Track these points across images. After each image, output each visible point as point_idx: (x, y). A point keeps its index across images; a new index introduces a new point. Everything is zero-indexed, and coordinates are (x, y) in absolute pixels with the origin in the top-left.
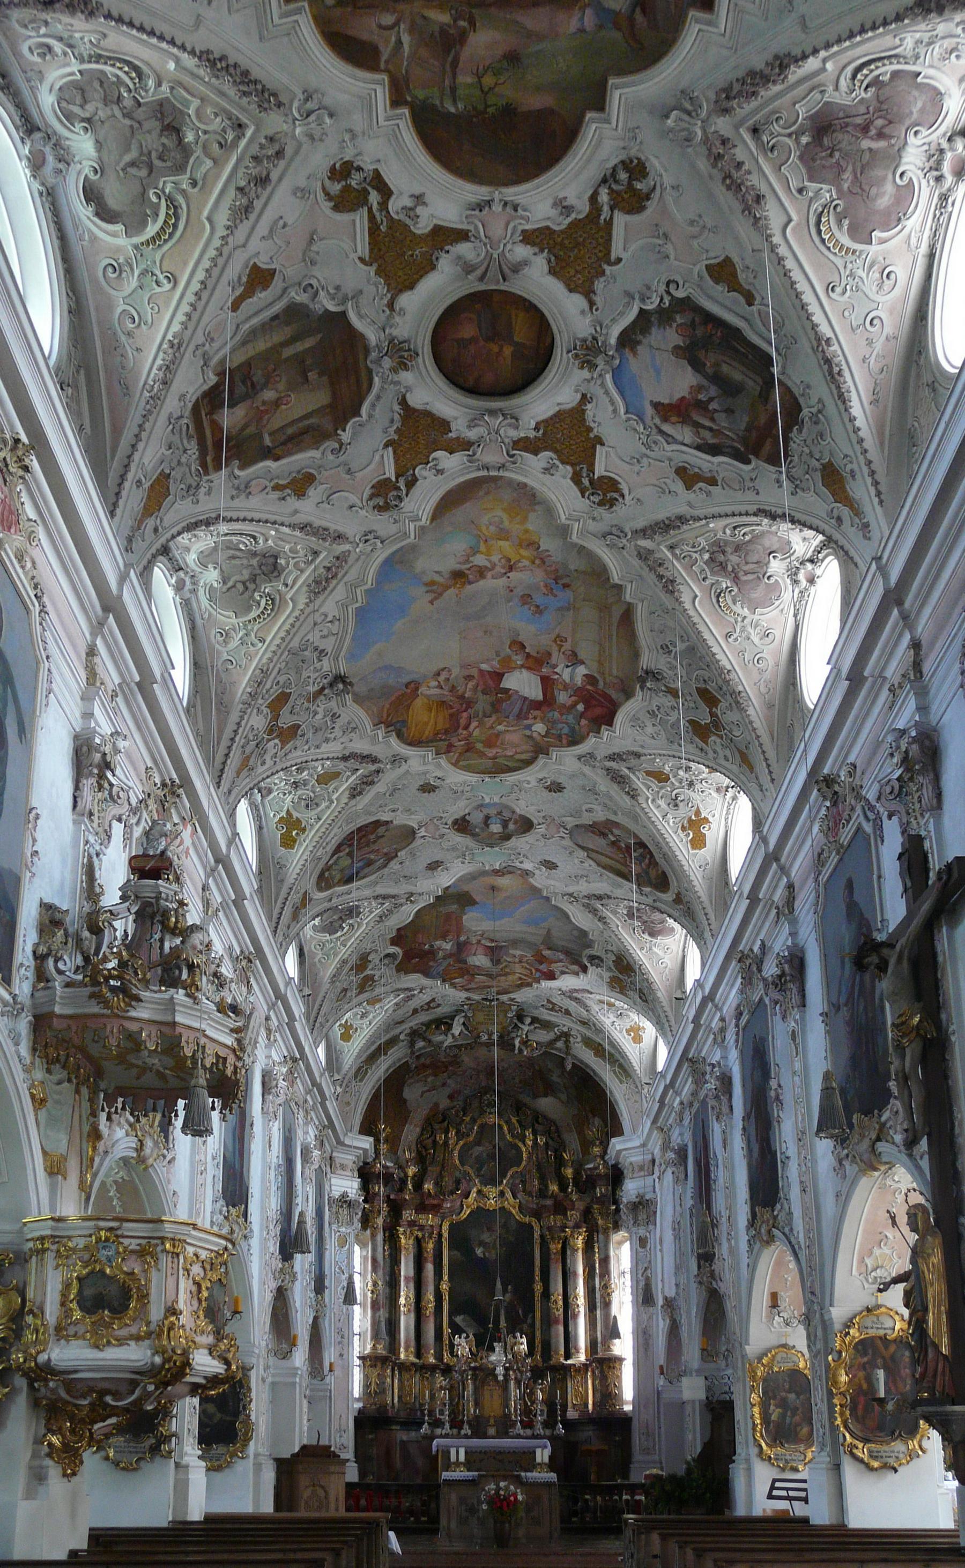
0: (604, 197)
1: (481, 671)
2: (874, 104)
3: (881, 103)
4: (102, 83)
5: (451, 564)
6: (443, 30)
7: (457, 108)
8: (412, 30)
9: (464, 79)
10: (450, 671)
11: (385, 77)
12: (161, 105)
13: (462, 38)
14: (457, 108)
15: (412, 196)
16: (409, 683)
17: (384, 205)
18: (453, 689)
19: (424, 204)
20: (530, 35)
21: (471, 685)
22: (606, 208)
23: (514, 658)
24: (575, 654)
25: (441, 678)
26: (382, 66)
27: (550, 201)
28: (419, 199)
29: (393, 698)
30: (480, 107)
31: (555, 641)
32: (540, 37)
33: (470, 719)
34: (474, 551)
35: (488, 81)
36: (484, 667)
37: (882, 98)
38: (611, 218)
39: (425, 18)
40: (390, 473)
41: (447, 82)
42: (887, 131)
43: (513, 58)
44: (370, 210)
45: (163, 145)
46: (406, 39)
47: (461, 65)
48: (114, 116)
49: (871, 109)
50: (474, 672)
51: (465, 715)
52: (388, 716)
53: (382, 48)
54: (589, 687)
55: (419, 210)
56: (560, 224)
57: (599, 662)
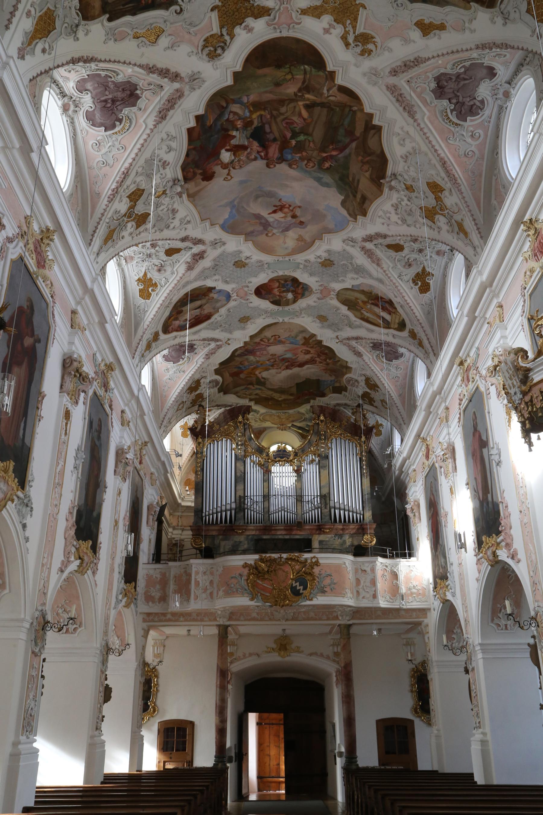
0: (227, 38)
2: (115, 111)
3: (113, 113)
4: (460, 112)
6: (308, 92)
7: (304, 67)
8: (322, 94)
9: (300, 77)
11: (336, 82)
12: (440, 96)
13: (300, 90)
14: (304, 67)
15: (331, 34)
17: (347, 33)
19: (324, 29)
20: (270, 92)
22: (225, 33)
26: (337, 86)
27: (255, 31)
28: (327, 31)
30: (292, 68)
32: (266, 92)
35: (289, 77)
37: (113, 114)
38: (221, 29)
39: (316, 97)
41: (308, 76)
42: (104, 103)
43: (277, 84)
44: (354, 33)
45: (447, 82)
46: (325, 91)
47: (301, 81)
48: (463, 97)
49: (116, 109)
53: (336, 91)
55: (327, 26)
56: (250, 21)
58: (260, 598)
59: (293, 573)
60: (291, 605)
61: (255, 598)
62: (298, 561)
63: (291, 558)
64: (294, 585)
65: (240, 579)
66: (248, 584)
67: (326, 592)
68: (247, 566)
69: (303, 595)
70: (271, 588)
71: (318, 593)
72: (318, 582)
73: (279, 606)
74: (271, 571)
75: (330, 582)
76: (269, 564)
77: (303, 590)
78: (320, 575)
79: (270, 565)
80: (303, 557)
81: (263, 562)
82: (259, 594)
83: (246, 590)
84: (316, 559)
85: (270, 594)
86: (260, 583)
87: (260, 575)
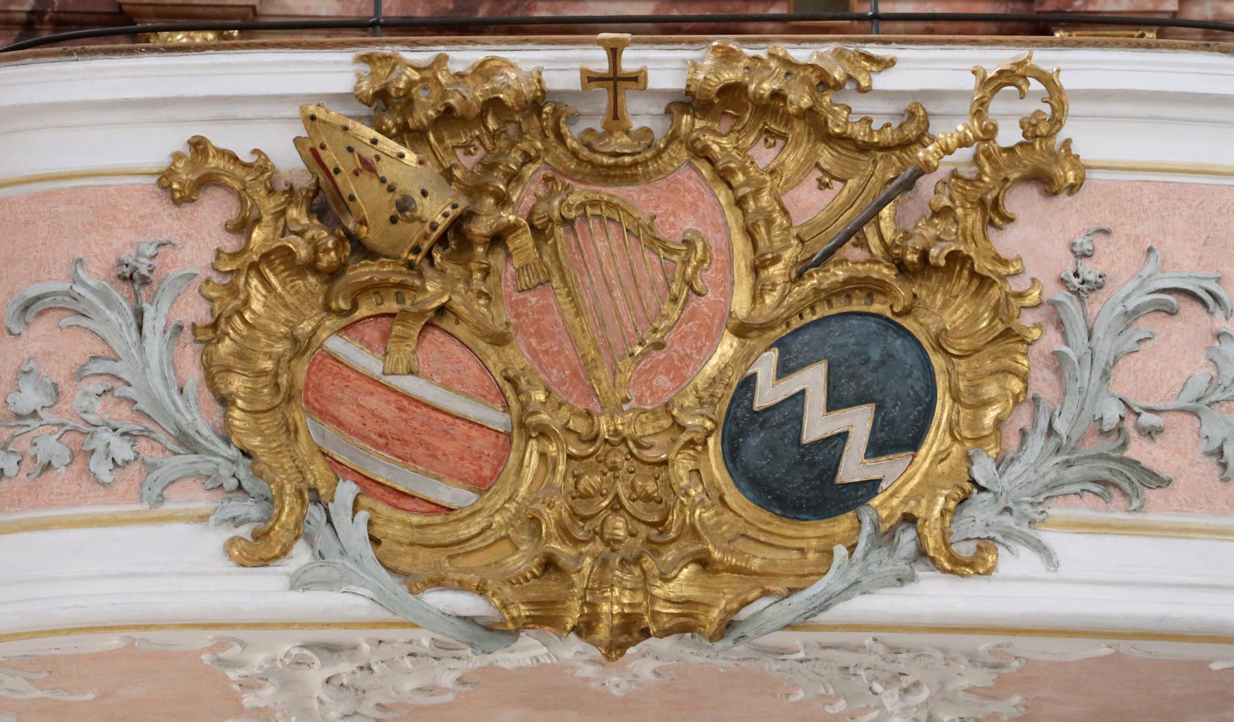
58: (355, 531)
59: (757, 269)
60: (728, 626)
61: (300, 531)
62: (813, 119)
63: (733, 92)
64: (768, 393)
65: (117, 321)
66: (212, 374)
67: (1161, 482)
68: (207, 181)
69: (883, 505)
70: (496, 418)
71: (1053, 489)
72: (1058, 362)
73: (585, 629)
74: (497, 239)
75: (1201, 374)
76: (467, 163)
77: (878, 448)
78: (1084, 289)
79: (489, 167)
80: (883, 81)
81: (408, 134)
82: (347, 490)
83: (186, 442)
84: (1035, 105)
85: (481, 486)
86: (370, 363)
87: (364, 271)
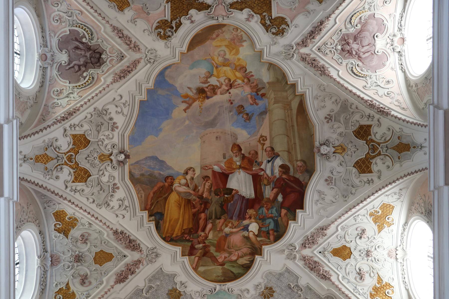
1: (214, 172)
5: (197, 84)
10: (194, 171)
16: (167, 177)
18: (195, 188)
21: (208, 184)
23: (235, 159)
24: (273, 149)
25: (188, 177)
29: (156, 188)
31: (259, 141)
33: (206, 220)
34: (210, 75)
36: (216, 168)
40: (168, 17)
50: (210, 174)
51: (203, 216)
52: (152, 205)
54: (284, 176)
57: (289, 152)
